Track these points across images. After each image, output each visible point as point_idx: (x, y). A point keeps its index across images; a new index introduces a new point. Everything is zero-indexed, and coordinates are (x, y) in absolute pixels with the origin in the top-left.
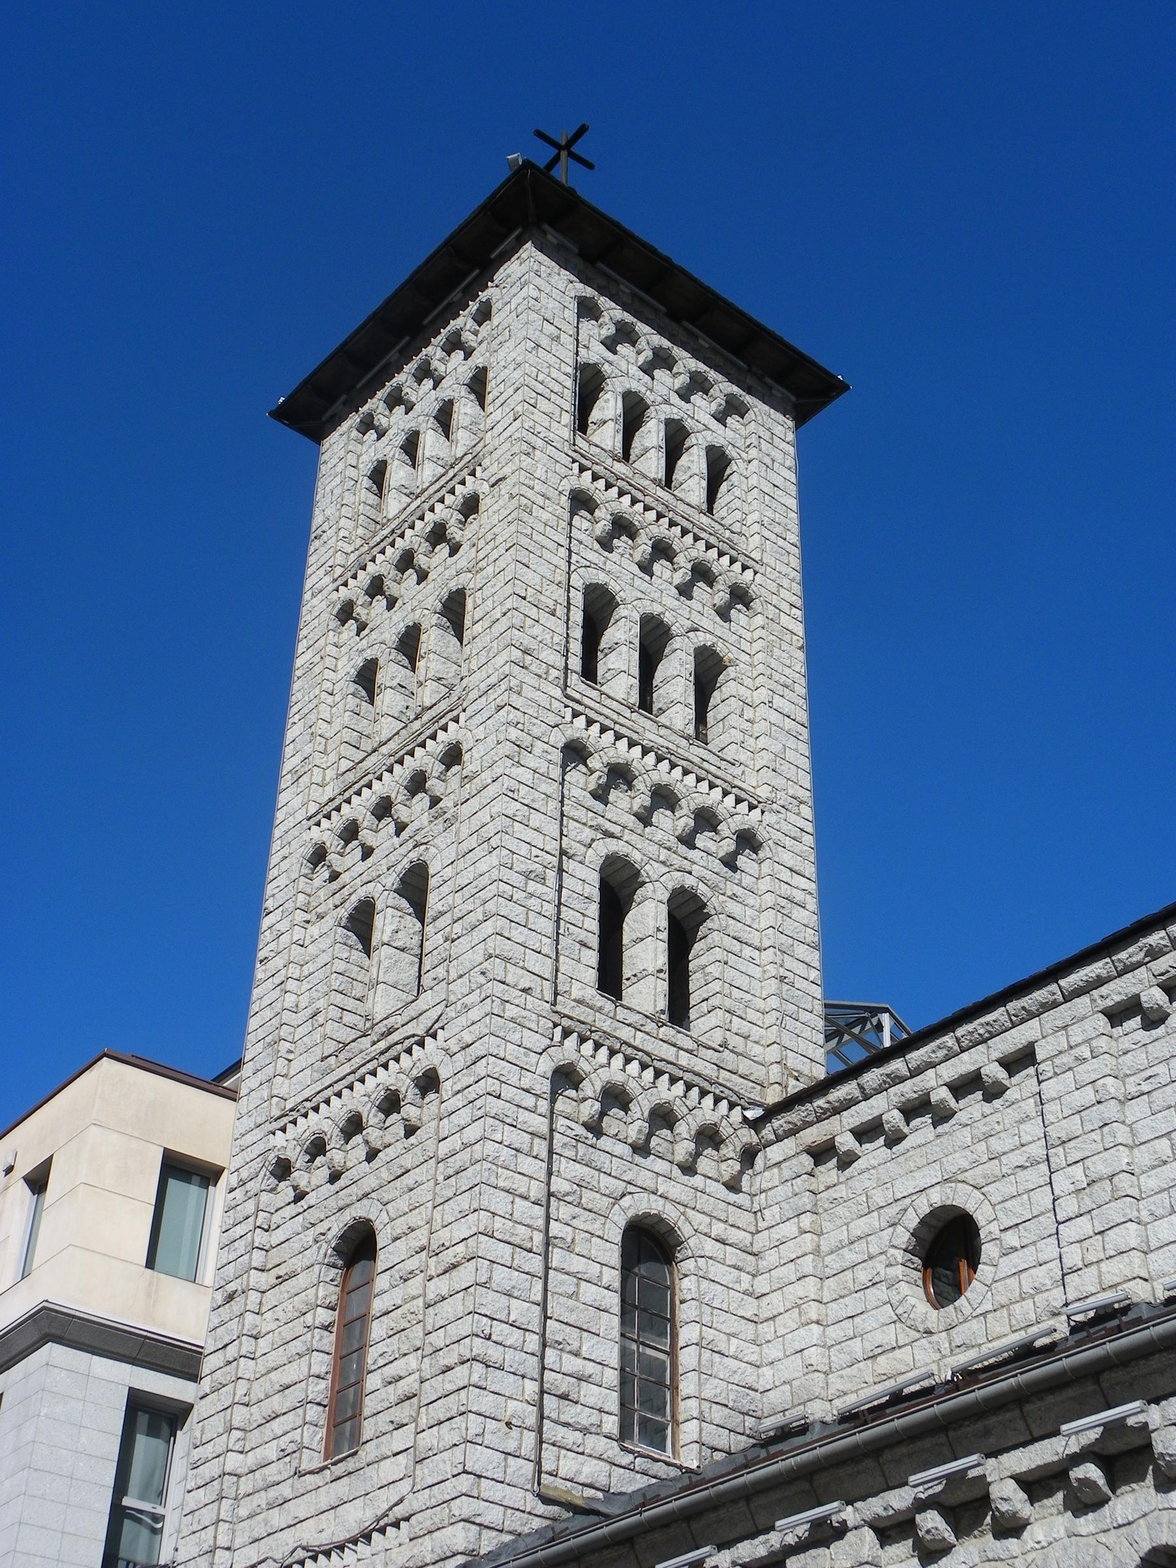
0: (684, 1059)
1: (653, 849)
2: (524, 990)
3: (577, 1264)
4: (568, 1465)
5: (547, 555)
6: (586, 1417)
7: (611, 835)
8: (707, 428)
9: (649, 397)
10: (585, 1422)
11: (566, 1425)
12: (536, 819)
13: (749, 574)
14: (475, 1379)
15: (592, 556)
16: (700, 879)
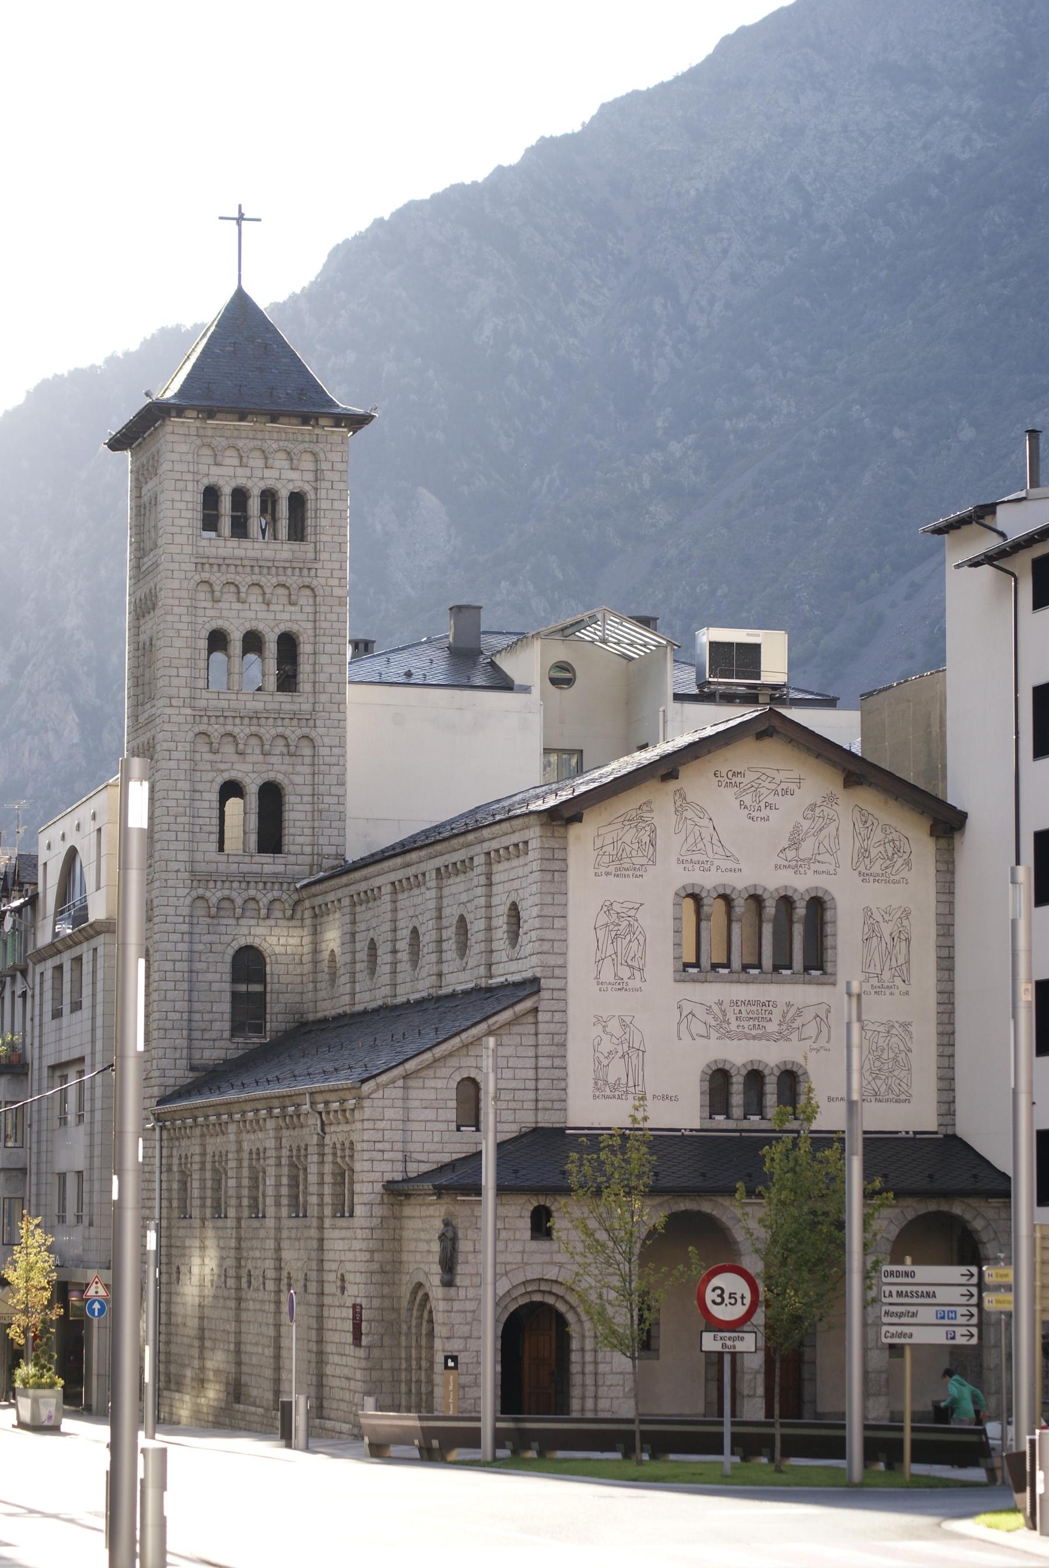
0: (267, 869)
1: (250, 768)
2: (176, 871)
3: (210, 977)
4: (207, 1054)
5: (183, 633)
6: (214, 1035)
7: (227, 770)
8: (290, 481)
9: (249, 484)
10: (214, 1037)
11: (207, 1040)
12: (180, 784)
13: (313, 572)
14: (160, 1036)
15: (210, 613)
16: (277, 772)
